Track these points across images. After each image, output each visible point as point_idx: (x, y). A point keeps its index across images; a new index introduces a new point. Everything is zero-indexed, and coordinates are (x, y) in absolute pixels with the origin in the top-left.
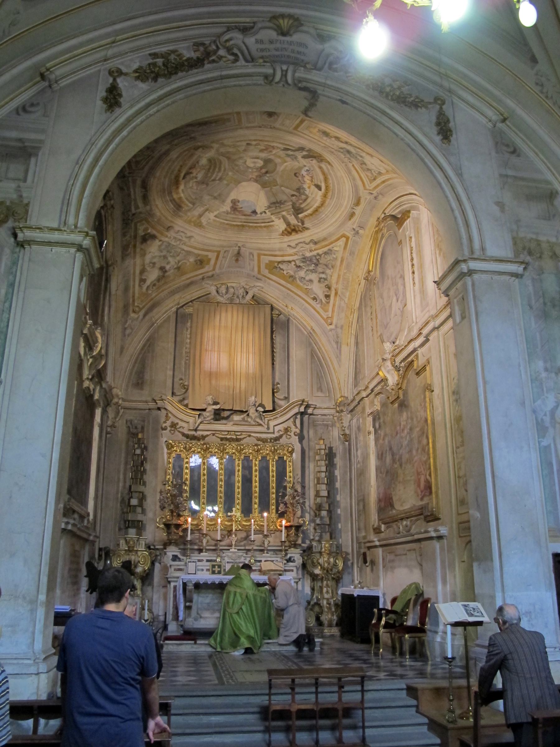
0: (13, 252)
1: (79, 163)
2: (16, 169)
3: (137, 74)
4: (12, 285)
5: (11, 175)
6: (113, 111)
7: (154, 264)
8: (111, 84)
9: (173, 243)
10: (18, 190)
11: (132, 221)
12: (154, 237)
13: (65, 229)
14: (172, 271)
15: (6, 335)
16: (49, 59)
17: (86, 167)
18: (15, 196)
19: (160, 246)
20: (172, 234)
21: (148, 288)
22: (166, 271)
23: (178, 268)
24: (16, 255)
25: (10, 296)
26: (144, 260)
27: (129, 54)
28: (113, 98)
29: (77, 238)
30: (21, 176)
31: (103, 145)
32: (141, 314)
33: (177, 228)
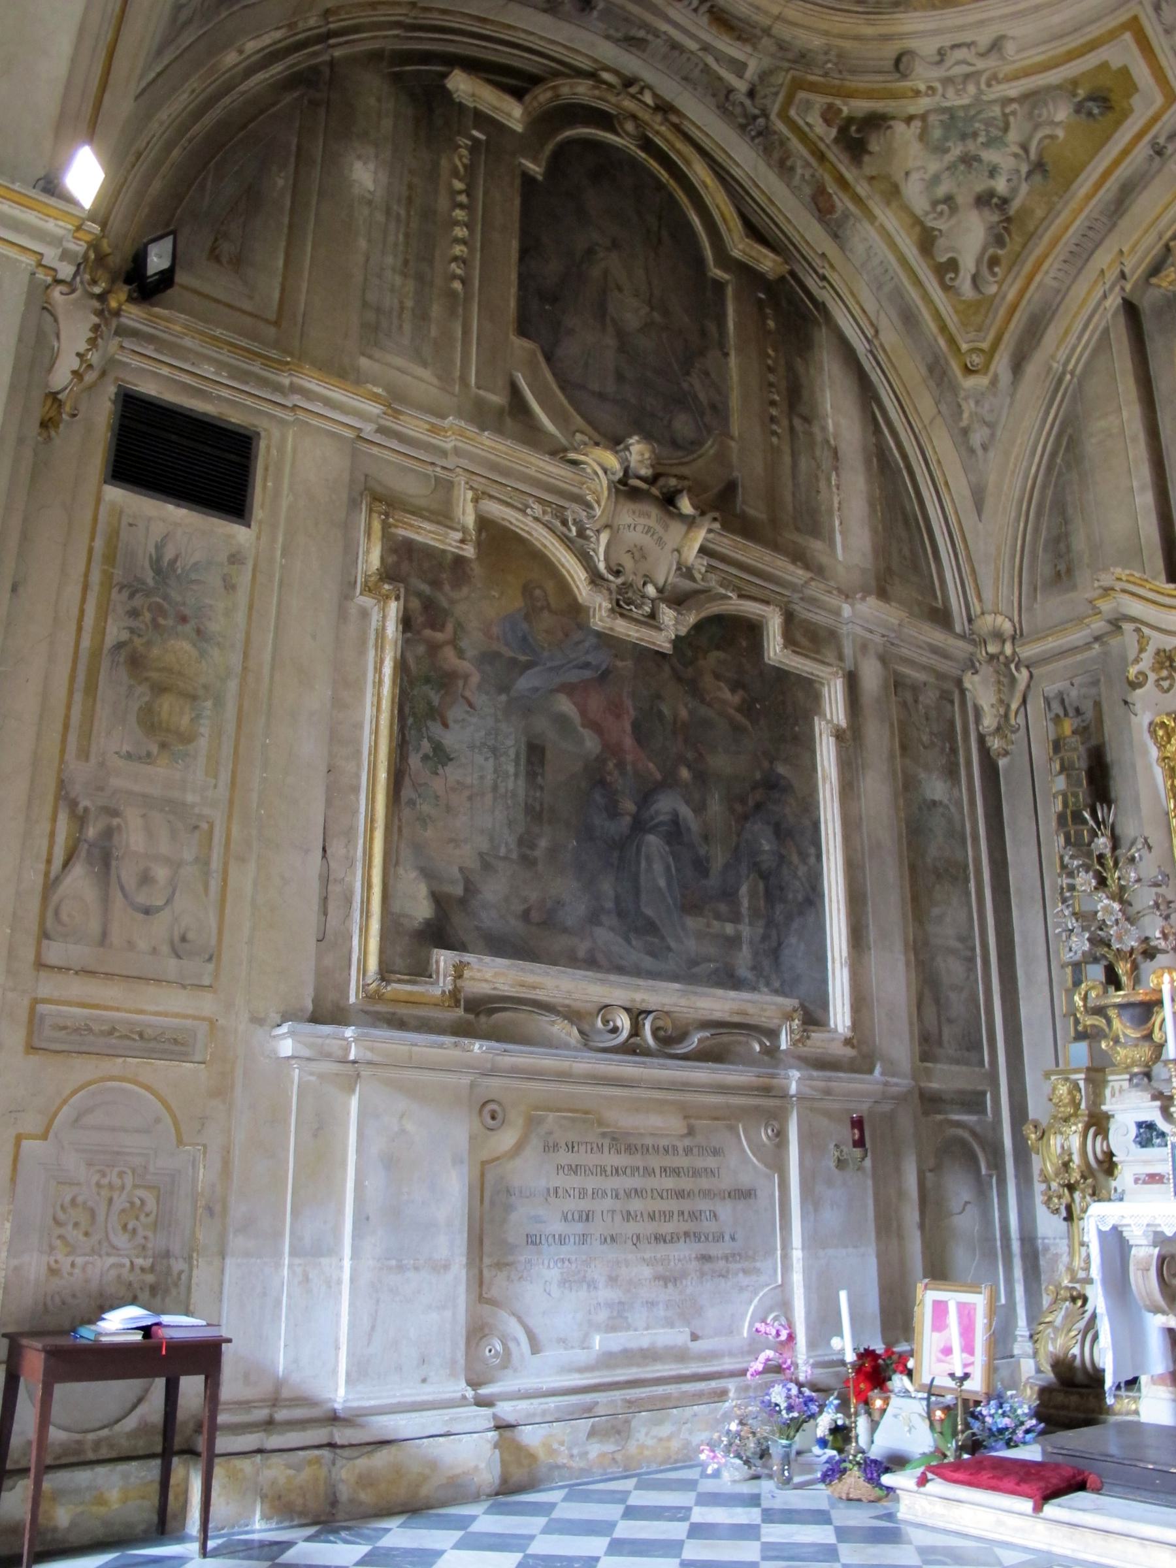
7: (949, 199)
9: (954, 100)
11: (765, 114)
12: (876, 122)
14: (1024, 188)
19: (923, 136)
20: (923, 75)
21: (975, 279)
22: (1005, 201)
23: (1039, 167)
26: (906, 209)
32: (1001, 364)
33: (927, 47)
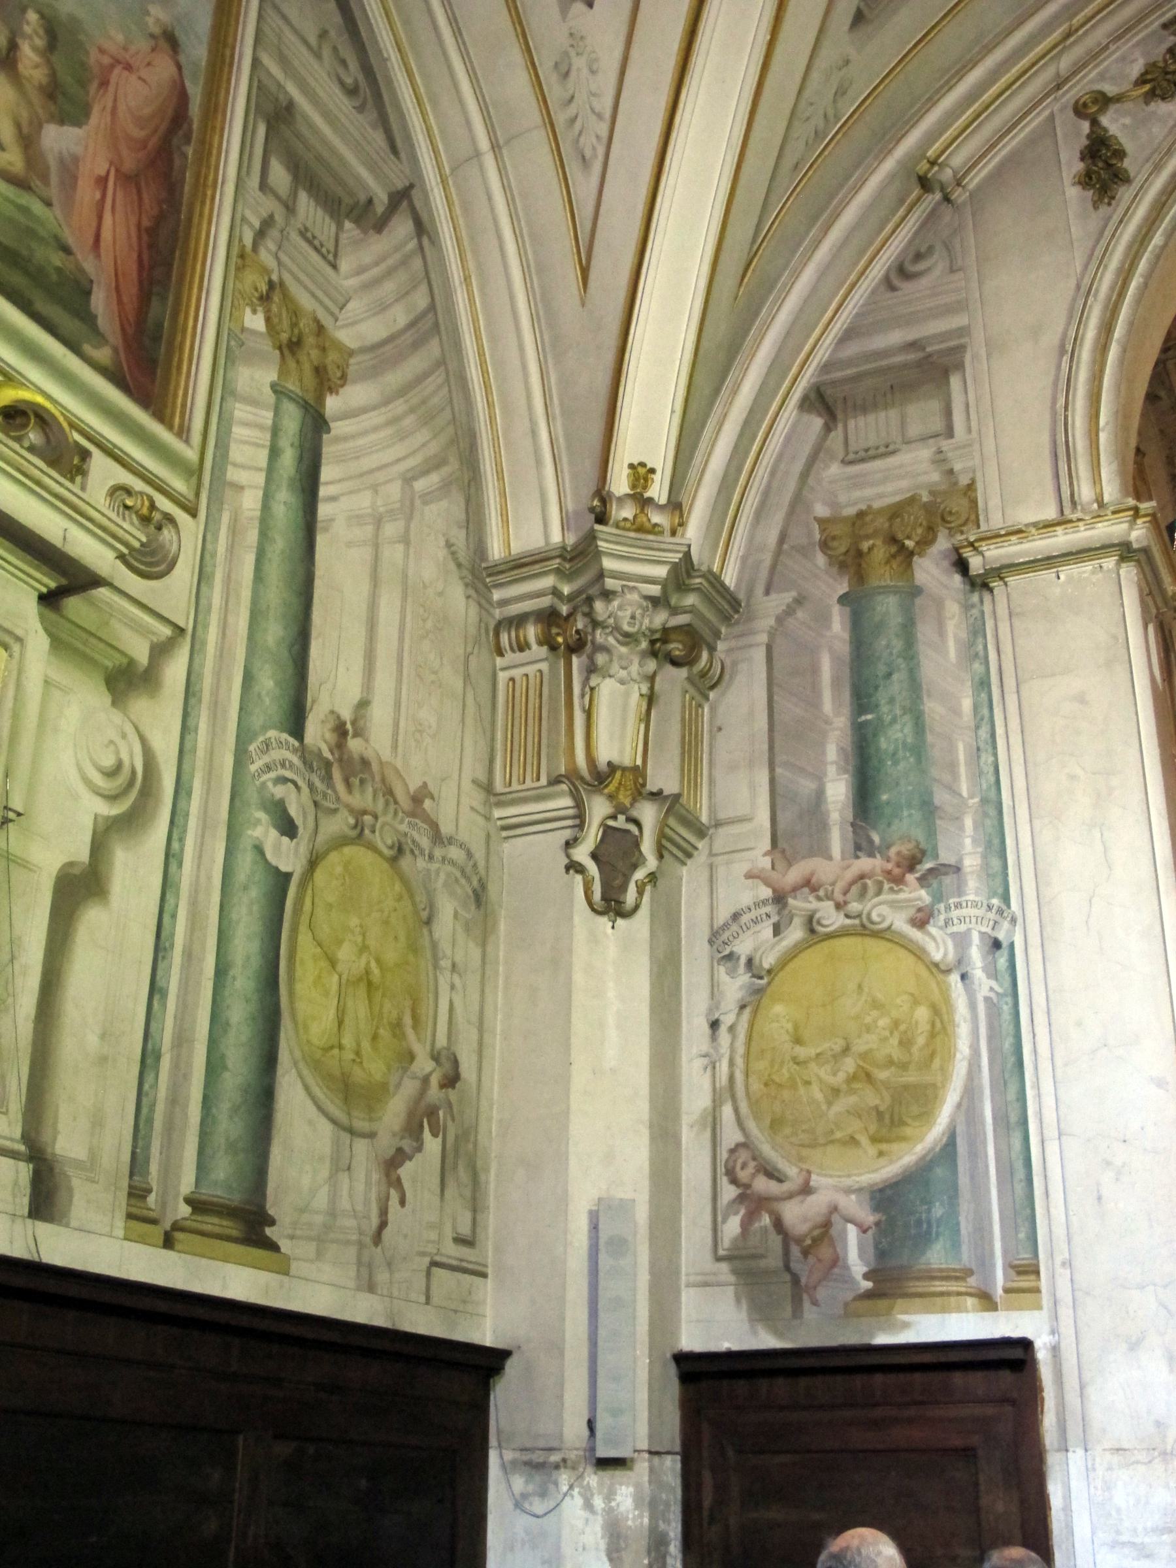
0: (967, 607)
1: (1067, 349)
2: (921, 414)
3: (1147, 87)
4: (983, 684)
5: (914, 430)
6: (1113, 198)
8: (1088, 137)
10: (940, 459)
13: (1079, 515)
15: (1000, 803)
16: (931, 137)
17: (1086, 353)
18: (935, 477)
24: (975, 612)
25: (985, 712)
27: (1112, 47)
28: (1103, 169)
29: (1112, 529)
30: (938, 425)
31: (1112, 289)
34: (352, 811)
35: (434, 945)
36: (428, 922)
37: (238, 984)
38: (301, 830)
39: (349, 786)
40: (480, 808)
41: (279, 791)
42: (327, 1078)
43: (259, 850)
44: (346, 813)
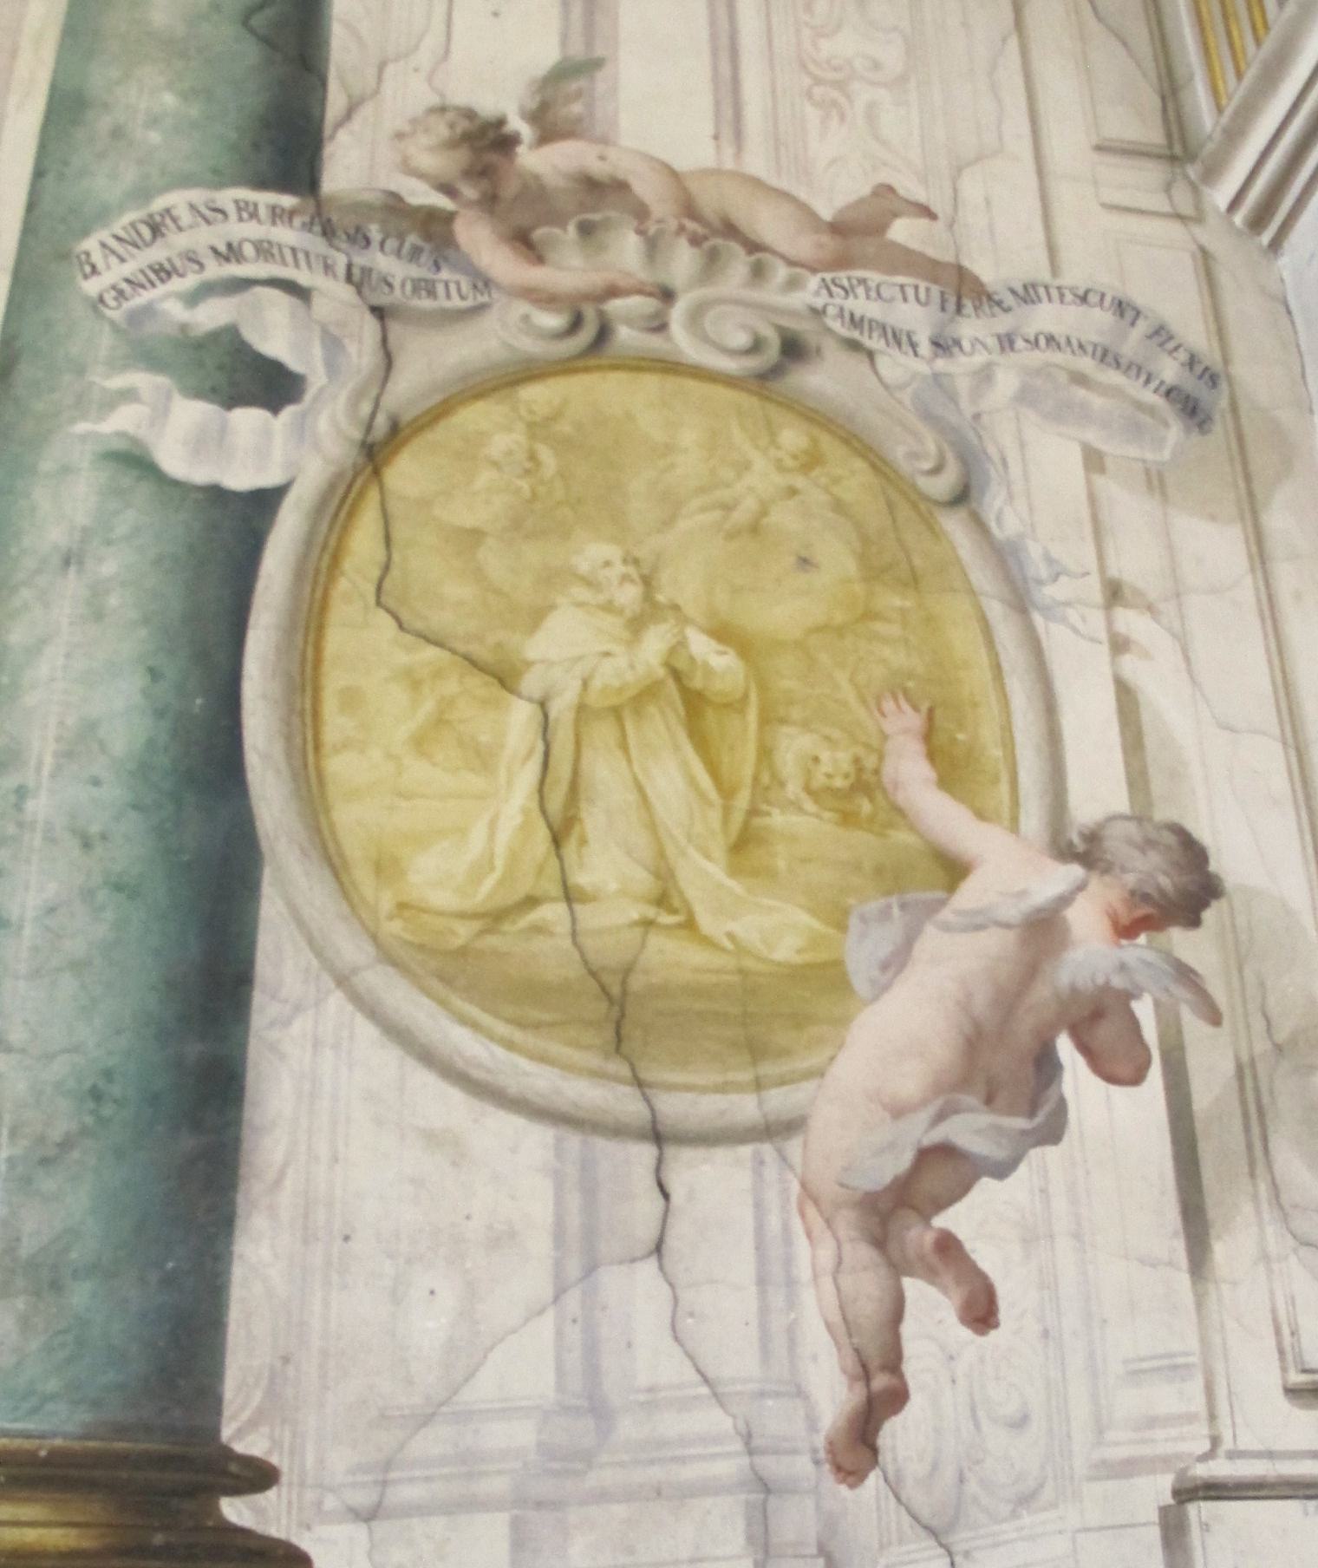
34: (546, 299)
35: (1004, 557)
36: (962, 497)
37: (39, 807)
38: (317, 379)
39: (525, 243)
40: (1159, 202)
41: (212, 315)
42: (521, 1000)
43: (133, 461)
44: (522, 307)
